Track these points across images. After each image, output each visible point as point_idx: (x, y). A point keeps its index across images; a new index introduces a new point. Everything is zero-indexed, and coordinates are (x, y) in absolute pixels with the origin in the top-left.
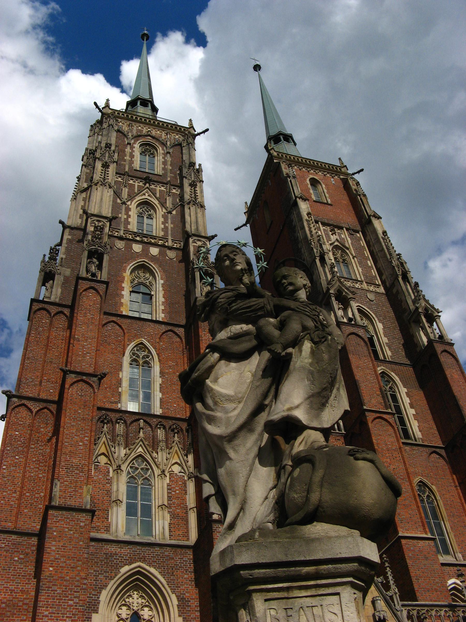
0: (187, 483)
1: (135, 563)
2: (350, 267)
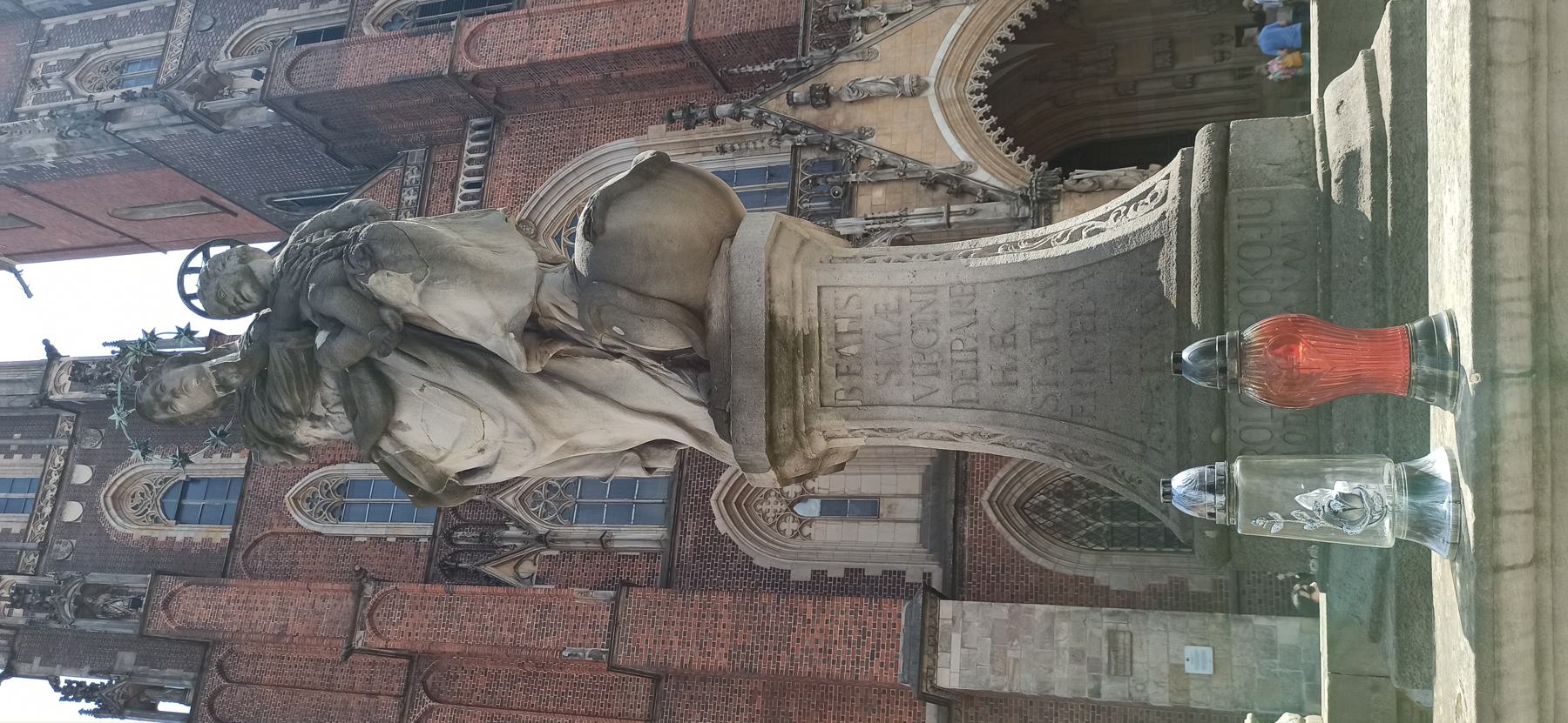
1: (711, 508)
2: (132, 57)
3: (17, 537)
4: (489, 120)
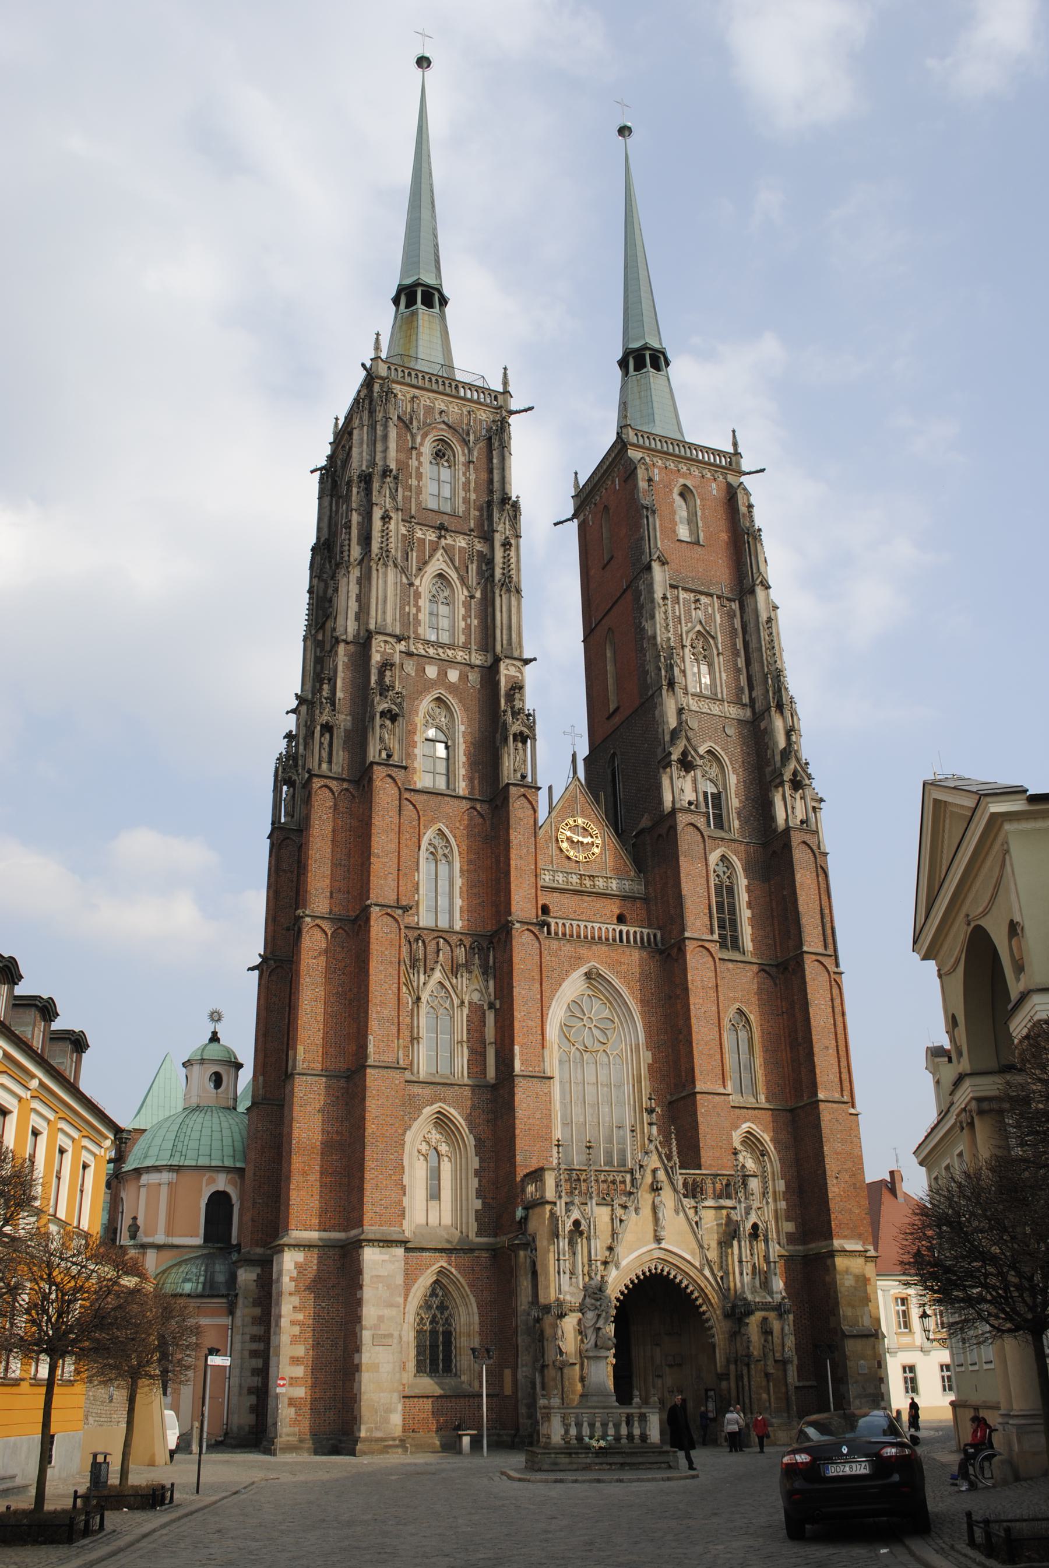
0: (487, 1012)
3: (416, 632)
4: (660, 945)
